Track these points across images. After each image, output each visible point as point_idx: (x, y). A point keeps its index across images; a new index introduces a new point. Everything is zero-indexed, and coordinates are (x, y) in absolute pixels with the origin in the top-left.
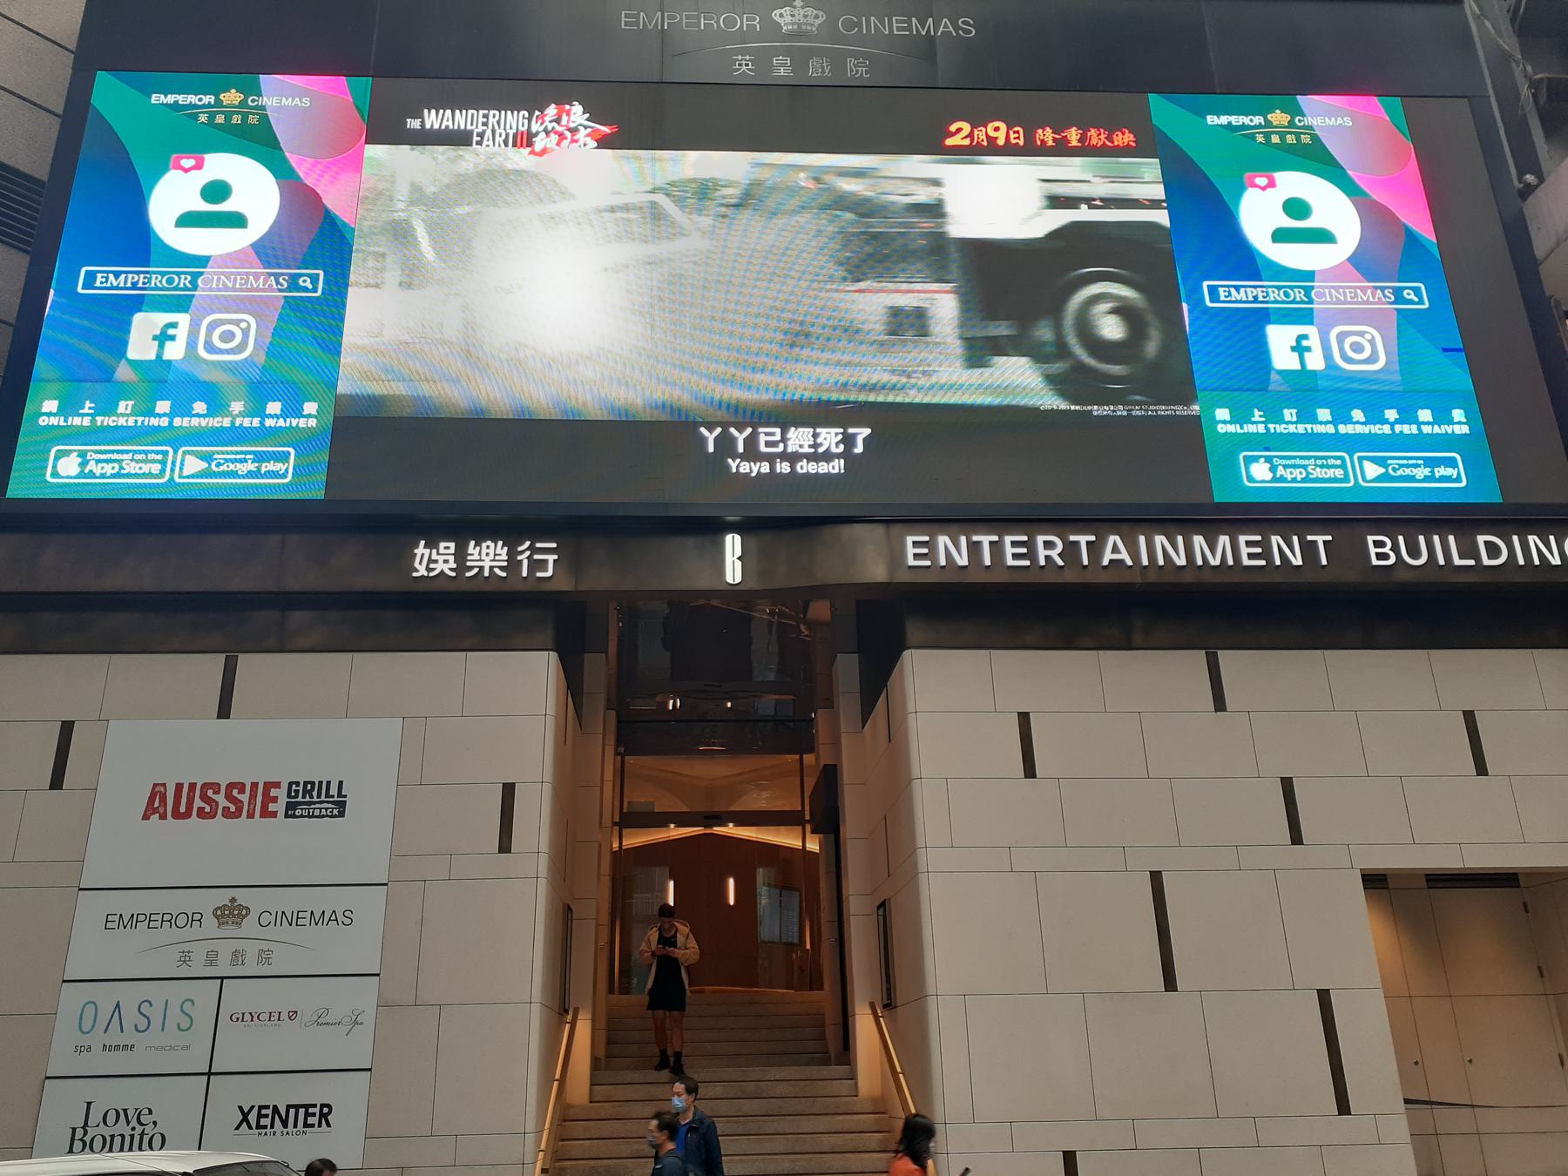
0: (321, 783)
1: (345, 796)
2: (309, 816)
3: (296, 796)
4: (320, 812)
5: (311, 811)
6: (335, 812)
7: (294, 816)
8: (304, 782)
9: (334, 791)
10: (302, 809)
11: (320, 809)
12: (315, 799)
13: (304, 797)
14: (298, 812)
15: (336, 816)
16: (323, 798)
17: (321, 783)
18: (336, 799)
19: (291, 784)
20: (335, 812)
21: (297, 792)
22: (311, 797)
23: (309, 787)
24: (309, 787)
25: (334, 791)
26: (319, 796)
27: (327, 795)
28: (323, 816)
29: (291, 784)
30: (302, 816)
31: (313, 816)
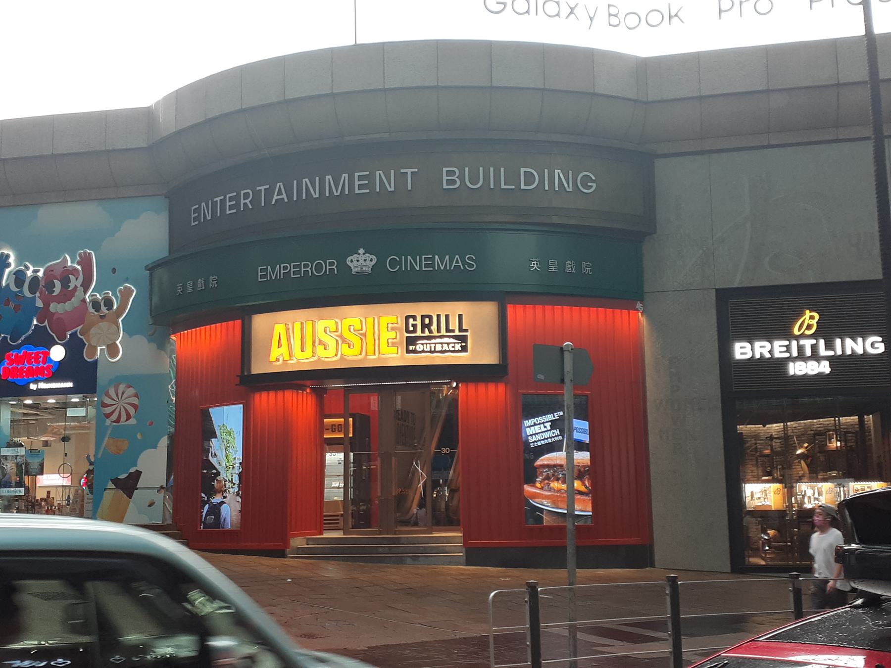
0: (438, 316)
1: (466, 331)
2: (431, 352)
3: (414, 331)
4: (442, 347)
5: (433, 346)
6: (458, 347)
7: (415, 351)
8: (422, 316)
9: (454, 324)
10: (422, 344)
11: (442, 343)
12: (435, 334)
13: (423, 331)
14: (419, 348)
15: (458, 351)
16: (443, 332)
17: (438, 316)
18: (457, 333)
19: (407, 318)
20: (458, 347)
21: (414, 326)
22: (430, 331)
23: (427, 321)
24: (427, 321)
25: (454, 324)
26: (439, 330)
27: (448, 330)
28: (445, 351)
29: (407, 318)
30: (423, 351)
31: (435, 352)
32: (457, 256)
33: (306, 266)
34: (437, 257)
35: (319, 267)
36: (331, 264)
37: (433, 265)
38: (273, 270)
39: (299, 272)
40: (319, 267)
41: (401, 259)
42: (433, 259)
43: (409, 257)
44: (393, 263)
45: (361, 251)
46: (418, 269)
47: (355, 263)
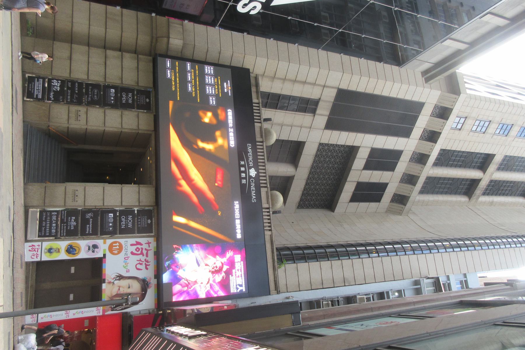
32: (255, 197)
33: (251, 158)
34: (255, 192)
35: (251, 161)
36: (252, 165)
37: (252, 191)
38: (250, 149)
39: (249, 156)
40: (251, 161)
41: (254, 183)
42: (254, 191)
43: (254, 185)
44: (252, 181)
45: (256, 173)
46: (251, 187)
47: (252, 171)
